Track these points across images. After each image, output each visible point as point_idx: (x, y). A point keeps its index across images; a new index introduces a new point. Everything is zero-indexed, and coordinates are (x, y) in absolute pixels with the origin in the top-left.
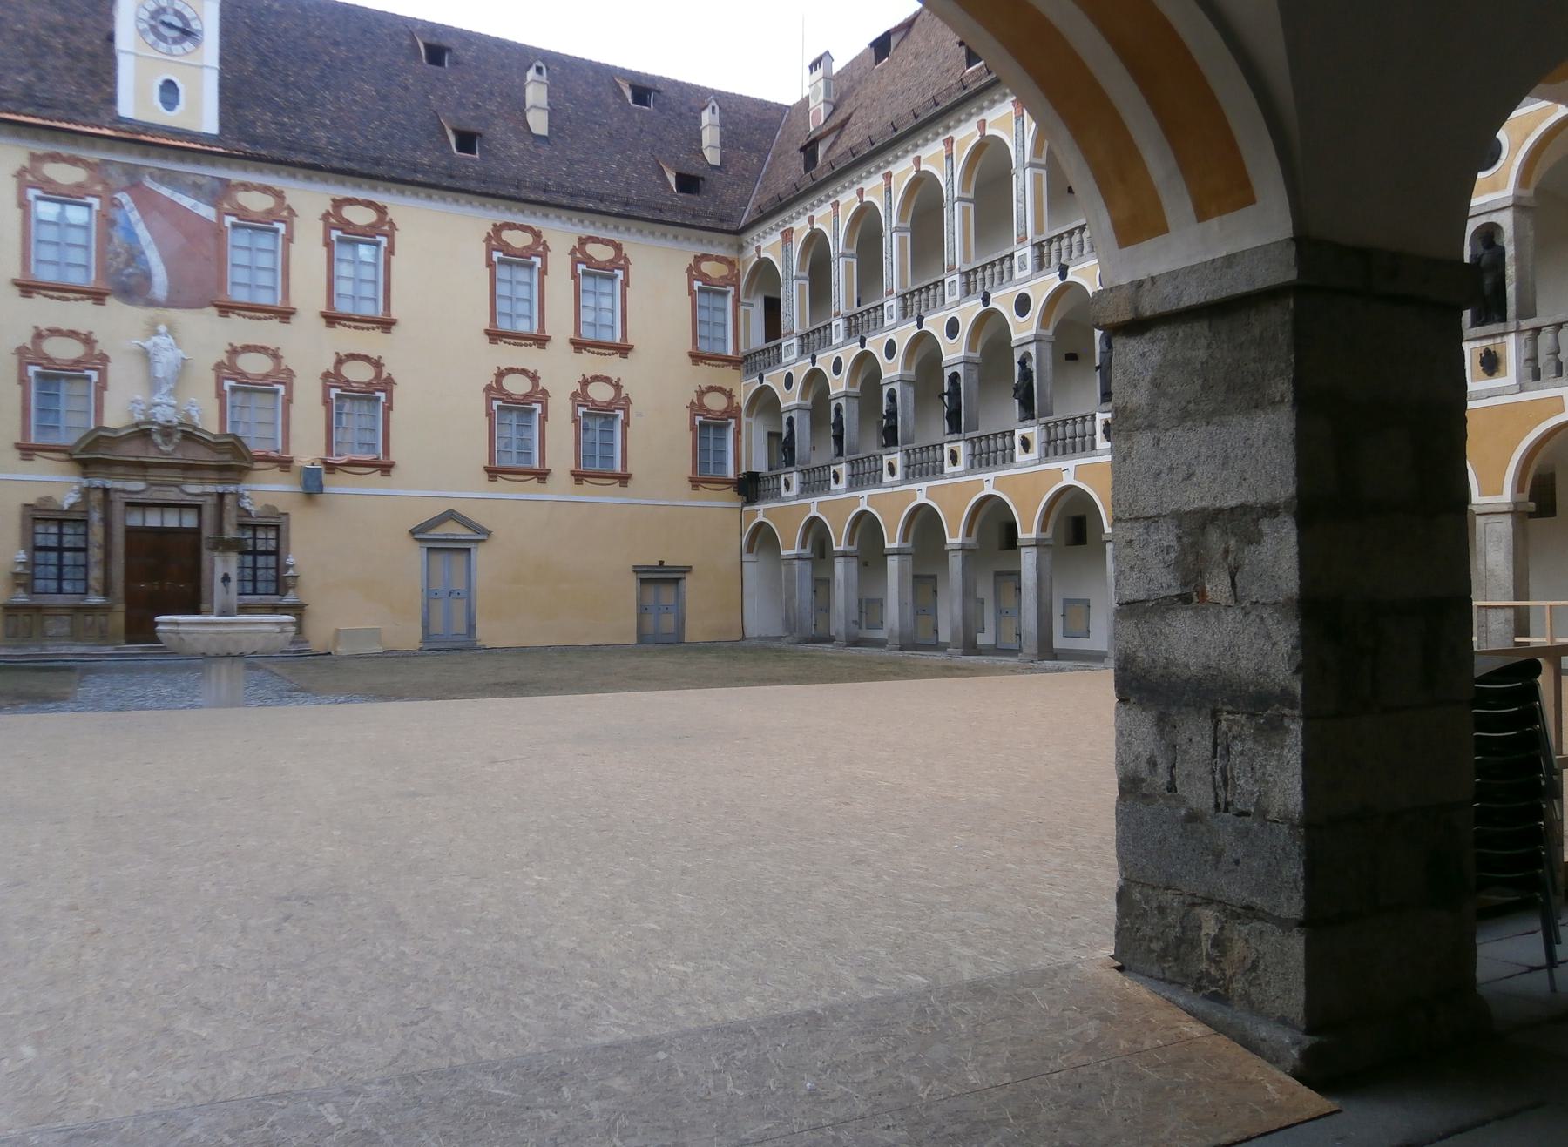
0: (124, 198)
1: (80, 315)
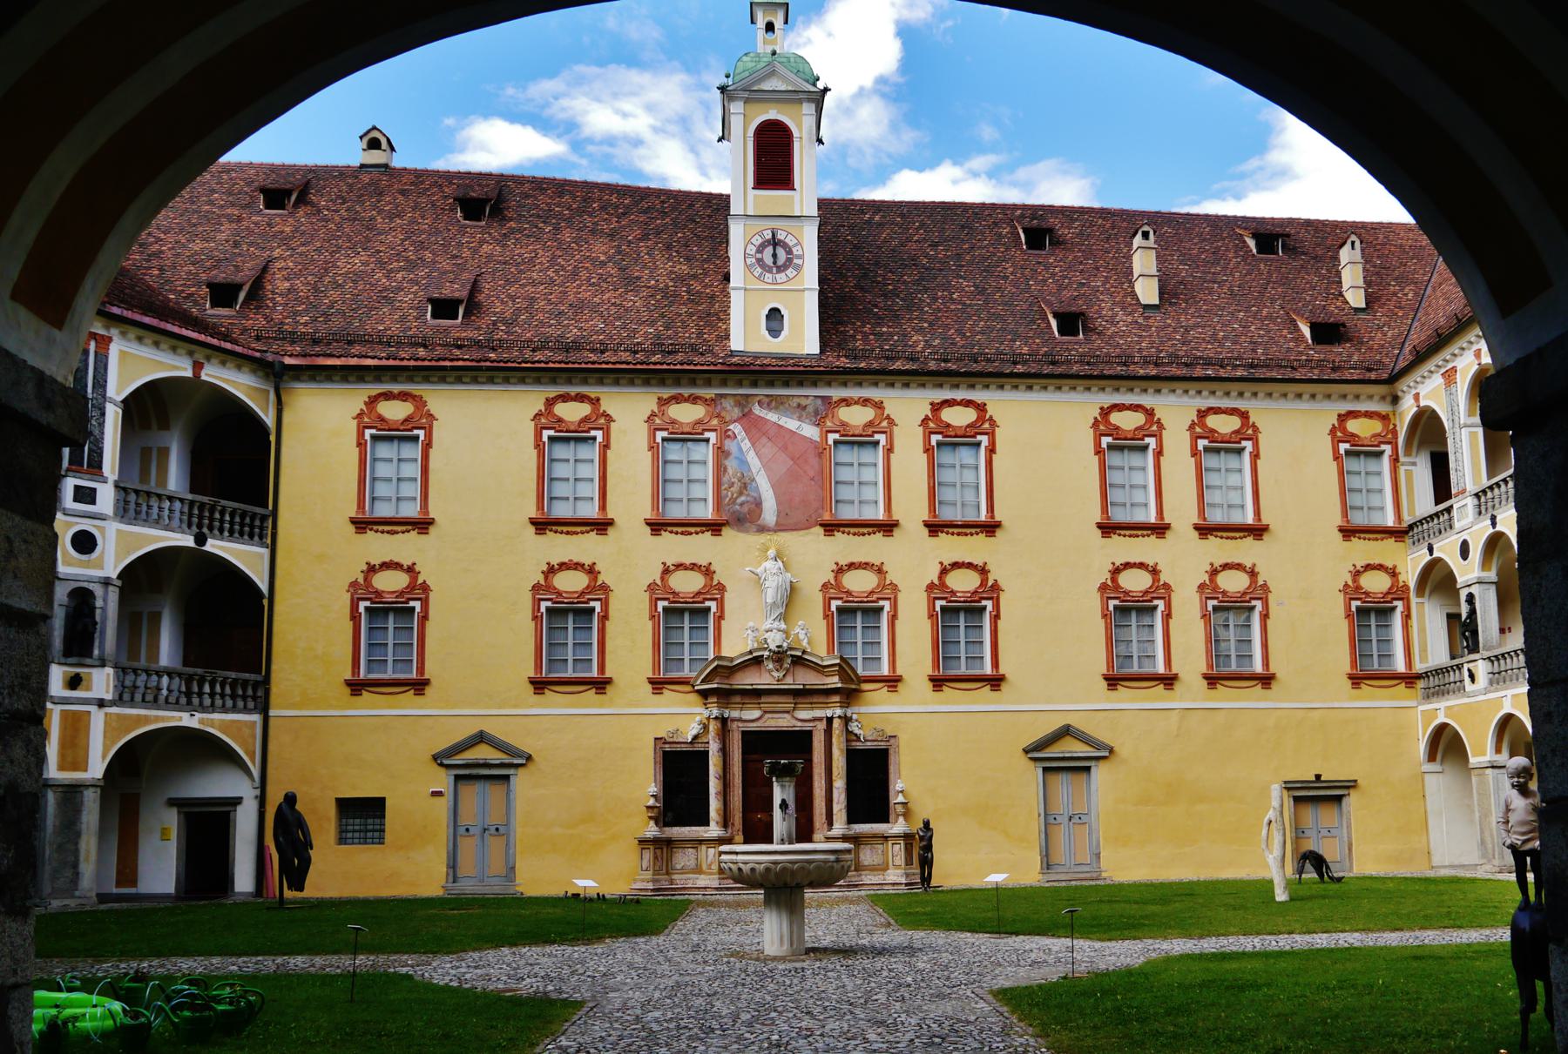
0: (736, 428)
1: (699, 547)
